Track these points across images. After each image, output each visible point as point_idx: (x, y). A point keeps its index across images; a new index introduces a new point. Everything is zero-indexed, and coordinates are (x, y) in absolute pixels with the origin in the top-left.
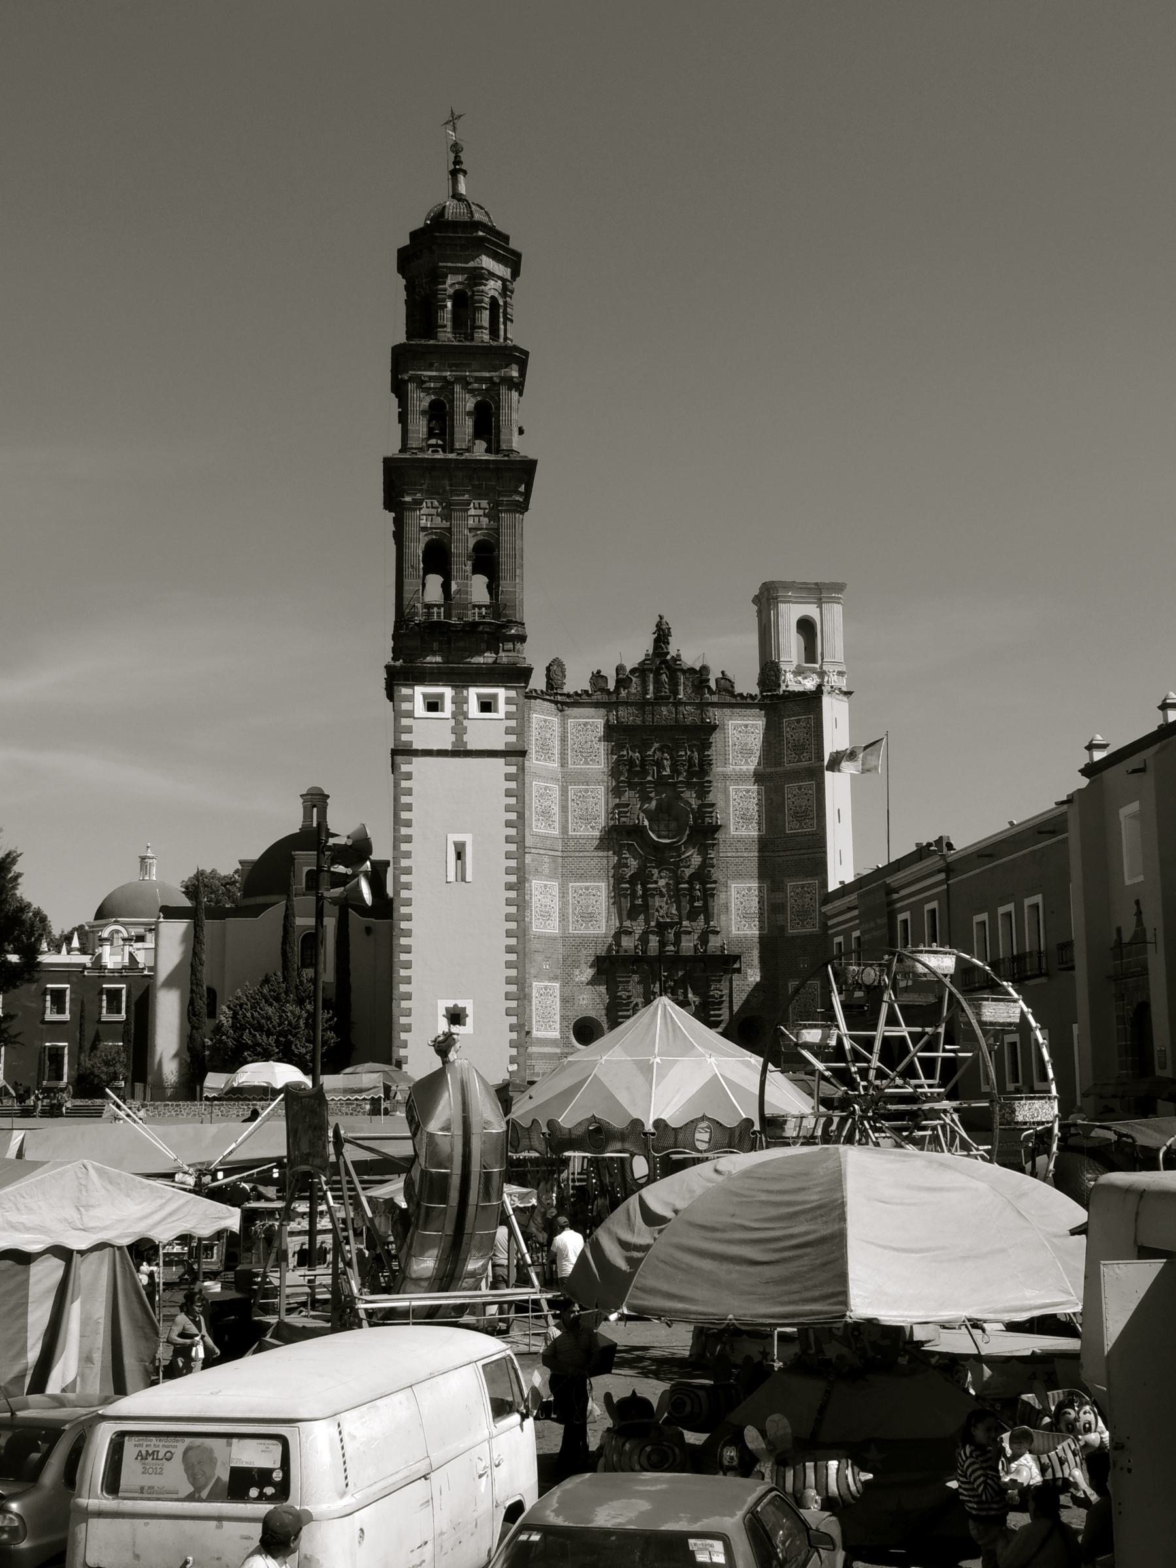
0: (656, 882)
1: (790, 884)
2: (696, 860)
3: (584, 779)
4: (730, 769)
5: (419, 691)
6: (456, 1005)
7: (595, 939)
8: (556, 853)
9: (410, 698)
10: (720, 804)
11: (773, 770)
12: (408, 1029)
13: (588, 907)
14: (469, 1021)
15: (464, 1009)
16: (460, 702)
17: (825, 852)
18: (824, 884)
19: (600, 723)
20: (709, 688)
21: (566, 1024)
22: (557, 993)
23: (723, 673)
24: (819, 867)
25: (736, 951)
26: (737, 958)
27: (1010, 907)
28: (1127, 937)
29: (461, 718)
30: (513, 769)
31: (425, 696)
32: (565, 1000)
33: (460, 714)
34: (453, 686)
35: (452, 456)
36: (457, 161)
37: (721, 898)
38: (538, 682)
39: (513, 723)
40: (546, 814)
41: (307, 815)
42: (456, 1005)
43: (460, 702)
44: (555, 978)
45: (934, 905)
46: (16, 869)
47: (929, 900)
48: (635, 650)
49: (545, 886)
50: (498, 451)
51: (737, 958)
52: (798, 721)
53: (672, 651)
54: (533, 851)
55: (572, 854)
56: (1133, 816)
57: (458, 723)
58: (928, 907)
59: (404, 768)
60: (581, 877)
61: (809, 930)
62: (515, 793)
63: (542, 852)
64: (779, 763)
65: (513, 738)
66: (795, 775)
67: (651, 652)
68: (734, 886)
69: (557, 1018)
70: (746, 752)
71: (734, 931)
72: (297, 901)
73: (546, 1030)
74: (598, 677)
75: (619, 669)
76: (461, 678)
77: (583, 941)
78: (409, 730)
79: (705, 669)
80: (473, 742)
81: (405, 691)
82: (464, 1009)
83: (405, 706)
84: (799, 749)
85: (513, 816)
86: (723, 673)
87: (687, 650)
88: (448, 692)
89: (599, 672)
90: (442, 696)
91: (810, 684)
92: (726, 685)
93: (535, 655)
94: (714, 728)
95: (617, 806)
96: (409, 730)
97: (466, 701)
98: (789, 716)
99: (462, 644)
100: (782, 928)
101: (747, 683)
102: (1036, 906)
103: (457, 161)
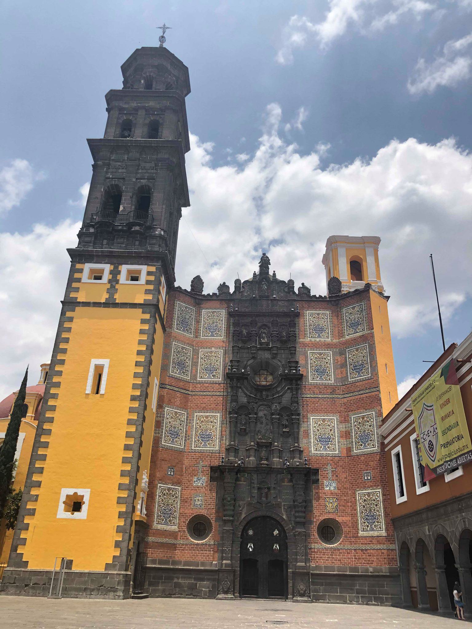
0: (256, 414)
2: (286, 399)
5: (87, 267)
6: (76, 493)
8: (187, 392)
9: (81, 271)
10: (302, 362)
12: (32, 513)
13: (207, 430)
14: (85, 508)
15: (83, 497)
16: (115, 273)
17: (379, 391)
18: (381, 414)
20: (294, 293)
21: (183, 519)
22: (179, 494)
23: (303, 284)
25: (314, 466)
26: (316, 472)
29: (114, 283)
30: (147, 316)
34: (111, 264)
39: (151, 287)
40: (181, 365)
42: (76, 493)
43: (115, 273)
44: (178, 483)
51: (316, 472)
52: (353, 308)
53: (271, 273)
54: (168, 387)
55: (199, 393)
57: (113, 287)
59: (69, 314)
60: (204, 410)
61: (369, 450)
63: (175, 389)
65: (150, 297)
66: (354, 342)
69: (177, 514)
70: (320, 330)
73: (166, 524)
74: (223, 287)
75: (237, 282)
77: (202, 455)
79: (291, 282)
80: (118, 298)
82: (83, 497)
83: (77, 275)
85: (144, 348)
86: (303, 284)
88: (107, 268)
89: (224, 283)
90: (102, 271)
92: (305, 289)
94: (297, 315)
95: (231, 361)
97: (119, 273)
98: (347, 306)
99: (122, 240)
100: (349, 450)
101: (320, 288)
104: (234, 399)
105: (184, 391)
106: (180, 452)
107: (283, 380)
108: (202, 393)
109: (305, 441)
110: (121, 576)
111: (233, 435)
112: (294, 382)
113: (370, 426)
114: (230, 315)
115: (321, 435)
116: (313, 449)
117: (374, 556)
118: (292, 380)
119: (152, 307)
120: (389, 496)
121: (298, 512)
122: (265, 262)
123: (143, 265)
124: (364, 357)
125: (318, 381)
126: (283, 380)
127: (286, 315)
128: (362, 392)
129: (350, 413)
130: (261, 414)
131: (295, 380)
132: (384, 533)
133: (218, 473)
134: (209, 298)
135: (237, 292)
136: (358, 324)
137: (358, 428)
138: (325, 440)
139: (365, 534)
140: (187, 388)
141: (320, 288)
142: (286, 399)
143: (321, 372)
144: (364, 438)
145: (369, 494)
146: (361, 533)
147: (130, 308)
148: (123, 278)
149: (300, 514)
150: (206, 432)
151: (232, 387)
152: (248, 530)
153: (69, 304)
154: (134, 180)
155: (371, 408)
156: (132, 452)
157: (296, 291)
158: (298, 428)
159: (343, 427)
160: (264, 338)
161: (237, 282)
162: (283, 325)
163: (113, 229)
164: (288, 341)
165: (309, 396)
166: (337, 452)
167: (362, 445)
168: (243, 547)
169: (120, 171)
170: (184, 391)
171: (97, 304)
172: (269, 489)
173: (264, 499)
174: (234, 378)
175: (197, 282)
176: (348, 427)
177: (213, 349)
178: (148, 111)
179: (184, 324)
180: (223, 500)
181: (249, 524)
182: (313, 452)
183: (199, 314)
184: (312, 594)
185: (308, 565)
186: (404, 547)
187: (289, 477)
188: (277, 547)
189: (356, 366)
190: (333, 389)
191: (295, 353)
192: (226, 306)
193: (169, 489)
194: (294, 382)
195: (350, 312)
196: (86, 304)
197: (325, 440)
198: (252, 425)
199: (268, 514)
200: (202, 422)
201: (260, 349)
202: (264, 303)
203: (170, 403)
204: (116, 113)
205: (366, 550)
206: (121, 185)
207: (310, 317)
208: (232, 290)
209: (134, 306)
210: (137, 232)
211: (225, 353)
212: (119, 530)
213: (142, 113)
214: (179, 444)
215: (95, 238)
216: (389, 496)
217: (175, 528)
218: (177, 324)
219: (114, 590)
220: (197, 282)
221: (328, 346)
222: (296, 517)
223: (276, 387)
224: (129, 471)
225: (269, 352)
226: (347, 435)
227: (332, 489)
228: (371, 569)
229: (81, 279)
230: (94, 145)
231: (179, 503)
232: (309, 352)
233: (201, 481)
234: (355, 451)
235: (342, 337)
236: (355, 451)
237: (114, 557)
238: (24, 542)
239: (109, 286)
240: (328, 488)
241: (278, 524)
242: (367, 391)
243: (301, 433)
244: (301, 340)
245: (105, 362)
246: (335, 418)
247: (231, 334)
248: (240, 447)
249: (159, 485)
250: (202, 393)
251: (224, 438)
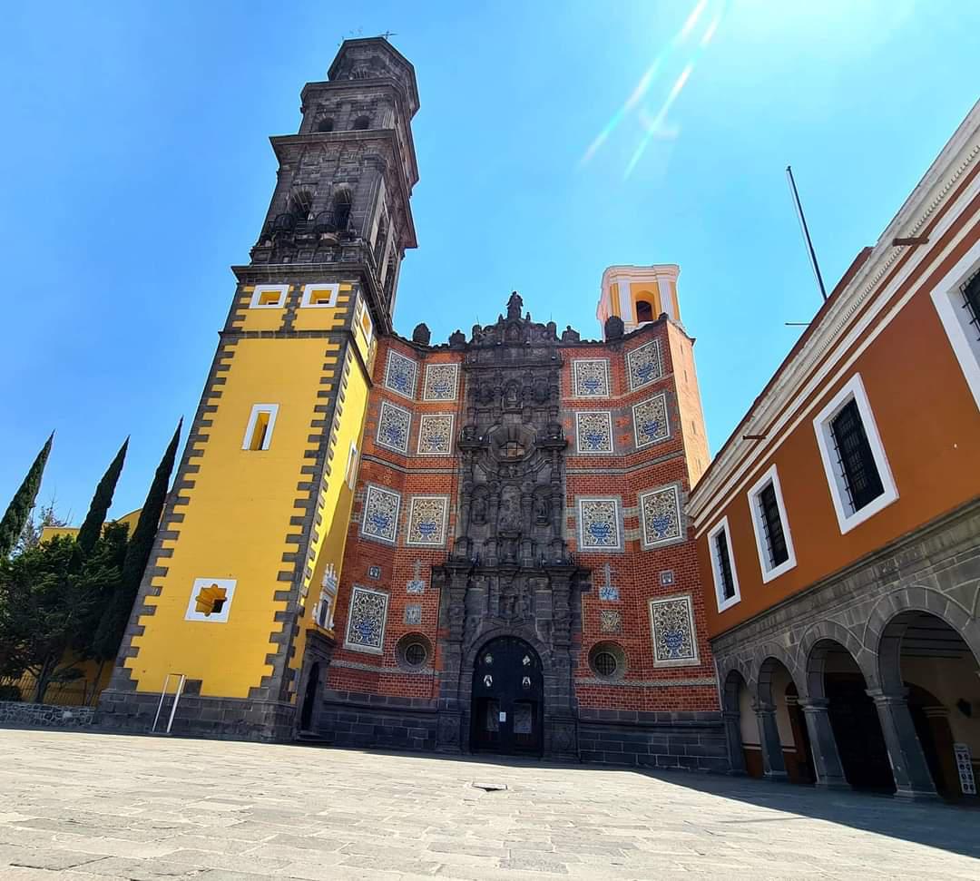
0: (499, 495)
1: (642, 496)
4: (575, 397)
5: (259, 290)
8: (401, 469)
9: (250, 295)
10: (566, 427)
11: (619, 397)
14: (226, 606)
19: (456, 366)
20: (556, 338)
23: (569, 327)
29: (293, 308)
30: (336, 347)
32: (395, 614)
34: (291, 283)
37: (568, 512)
40: (394, 433)
43: (295, 296)
44: (386, 588)
48: (491, 313)
49: (384, 495)
52: (642, 350)
53: (524, 316)
54: (374, 459)
59: (228, 348)
60: (425, 491)
61: (668, 540)
62: (333, 367)
63: (384, 463)
64: (623, 388)
67: (505, 317)
70: (592, 385)
71: (582, 547)
74: (457, 337)
75: (476, 328)
77: (420, 553)
79: (552, 326)
83: (243, 300)
84: (644, 372)
85: (328, 387)
86: (569, 327)
87: (536, 312)
88: (284, 289)
89: (458, 331)
92: (571, 334)
94: (561, 365)
98: (632, 349)
100: (637, 543)
101: (593, 331)
104: (470, 475)
105: (398, 468)
106: (388, 549)
107: (539, 451)
108: (423, 471)
109: (570, 532)
110: (272, 707)
111: (465, 524)
112: (555, 452)
113: (670, 506)
114: (464, 369)
115: (592, 523)
116: (582, 543)
117: (680, 696)
118: (552, 451)
121: (560, 630)
122: (515, 302)
123: (333, 282)
124: (658, 412)
125: (590, 451)
126: (539, 451)
127: (544, 364)
128: (656, 461)
129: (638, 493)
130: (506, 497)
131: (555, 446)
134: (437, 349)
135: (476, 341)
136: (649, 369)
137: (651, 511)
138: (600, 531)
139: (665, 663)
140: (402, 464)
142: (543, 476)
143: (594, 439)
144: (661, 524)
145: (669, 605)
147: (312, 337)
149: (563, 633)
150: (431, 520)
151: (465, 461)
152: (485, 655)
154: (330, 183)
155: (669, 480)
156: (301, 527)
158: (561, 514)
159: (630, 512)
160: (512, 397)
162: (541, 379)
163: (296, 240)
164: (546, 397)
165: (576, 471)
166: (619, 547)
167: (657, 535)
168: (477, 679)
169: (312, 176)
170: (398, 468)
171: (266, 334)
172: (516, 598)
173: (509, 612)
175: (422, 332)
176: (636, 512)
177: (440, 414)
178: (353, 103)
179: (399, 379)
180: (449, 610)
181: (487, 647)
182: (582, 547)
183: (422, 369)
184: (579, 751)
185: (575, 707)
187: (547, 580)
188: (527, 680)
189: (647, 426)
190: (612, 462)
191: (557, 415)
192: (459, 358)
193: (370, 596)
194: (555, 452)
195: (636, 357)
196: (253, 335)
197: (600, 531)
198: (493, 510)
199: (516, 633)
200: (422, 508)
201: (507, 412)
202: (514, 351)
203: (375, 479)
204: (313, 110)
205: (666, 688)
206: (312, 192)
207: (579, 365)
208: (468, 340)
209: (317, 334)
210: (329, 243)
211: (457, 418)
213: (347, 108)
214: (388, 537)
215: (274, 255)
218: (389, 380)
220: (422, 332)
221: (604, 404)
222: (556, 638)
223: (530, 460)
224: (294, 554)
225: (520, 416)
226: (633, 523)
227: (611, 598)
228: (674, 716)
229: (249, 304)
230: (280, 145)
231: (385, 616)
232: (577, 413)
233: (417, 586)
234: (647, 545)
235: (626, 391)
236: (646, 544)
237: (264, 678)
239: (285, 311)
240: (605, 598)
241: (529, 649)
242: (665, 458)
243: (565, 520)
244: (564, 399)
245: (273, 409)
246: (615, 500)
247: (465, 395)
248: (474, 541)
249: (355, 588)
250: (423, 471)
251: (453, 530)
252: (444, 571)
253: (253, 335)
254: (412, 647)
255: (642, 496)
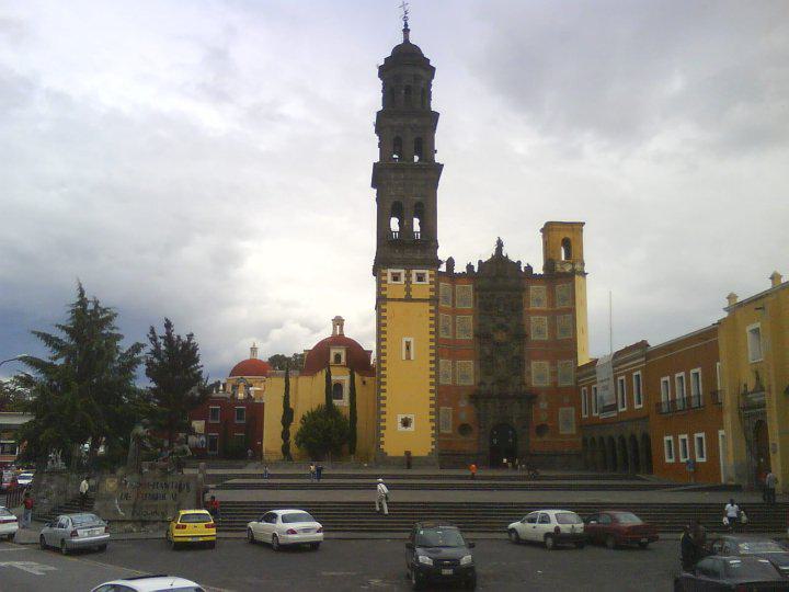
1: (559, 362)
3: (462, 312)
4: (531, 308)
5: (390, 271)
7: (471, 386)
9: (386, 275)
14: (413, 425)
16: (408, 276)
24: (573, 354)
27: (682, 374)
28: (751, 388)
30: (433, 308)
31: (393, 274)
32: (455, 416)
33: (408, 282)
35: (405, 162)
36: (406, 25)
37: (527, 369)
38: (443, 268)
41: (335, 327)
43: (408, 276)
45: (639, 372)
46: (198, 353)
47: (637, 370)
50: (426, 160)
56: (756, 332)
58: (636, 373)
59: (383, 307)
60: (463, 358)
68: (533, 363)
70: (539, 301)
72: (332, 369)
74: (470, 267)
75: (480, 262)
76: (409, 265)
78: (385, 289)
79: (519, 262)
81: (383, 271)
84: (564, 299)
85: (433, 330)
87: (512, 253)
88: (403, 272)
91: (568, 268)
92: (529, 268)
93: (442, 254)
94: (524, 290)
96: (385, 289)
100: (555, 383)
101: (538, 269)
102: (697, 374)
103: (406, 25)
114: (476, 290)
119: (434, 300)
120: (578, 414)
122: (500, 245)
125: (536, 338)
132: (574, 432)
133: (475, 398)
134: (460, 275)
141: (538, 269)
143: (540, 332)
146: (561, 432)
148: (414, 278)
153: (381, 299)
155: (570, 359)
157: (523, 270)
161: (480, 262)
174: (482, 336)
175: (451, 262)
186: (585, 441)
188: (511, 440)
195: (560, 289)
196: (393, 300)
208: (476, 270)
212: (433, 436)
214: (449, 382)
216: (578, 414)
217: (450, 432)
219: (434, 465)
226: (554, 374)
233: (464, 404)
238: (383, 443)
246: (546, 364)
252: (475, 398)
253: (393, 300)
254: (464, 429)
255: (559, 362)
